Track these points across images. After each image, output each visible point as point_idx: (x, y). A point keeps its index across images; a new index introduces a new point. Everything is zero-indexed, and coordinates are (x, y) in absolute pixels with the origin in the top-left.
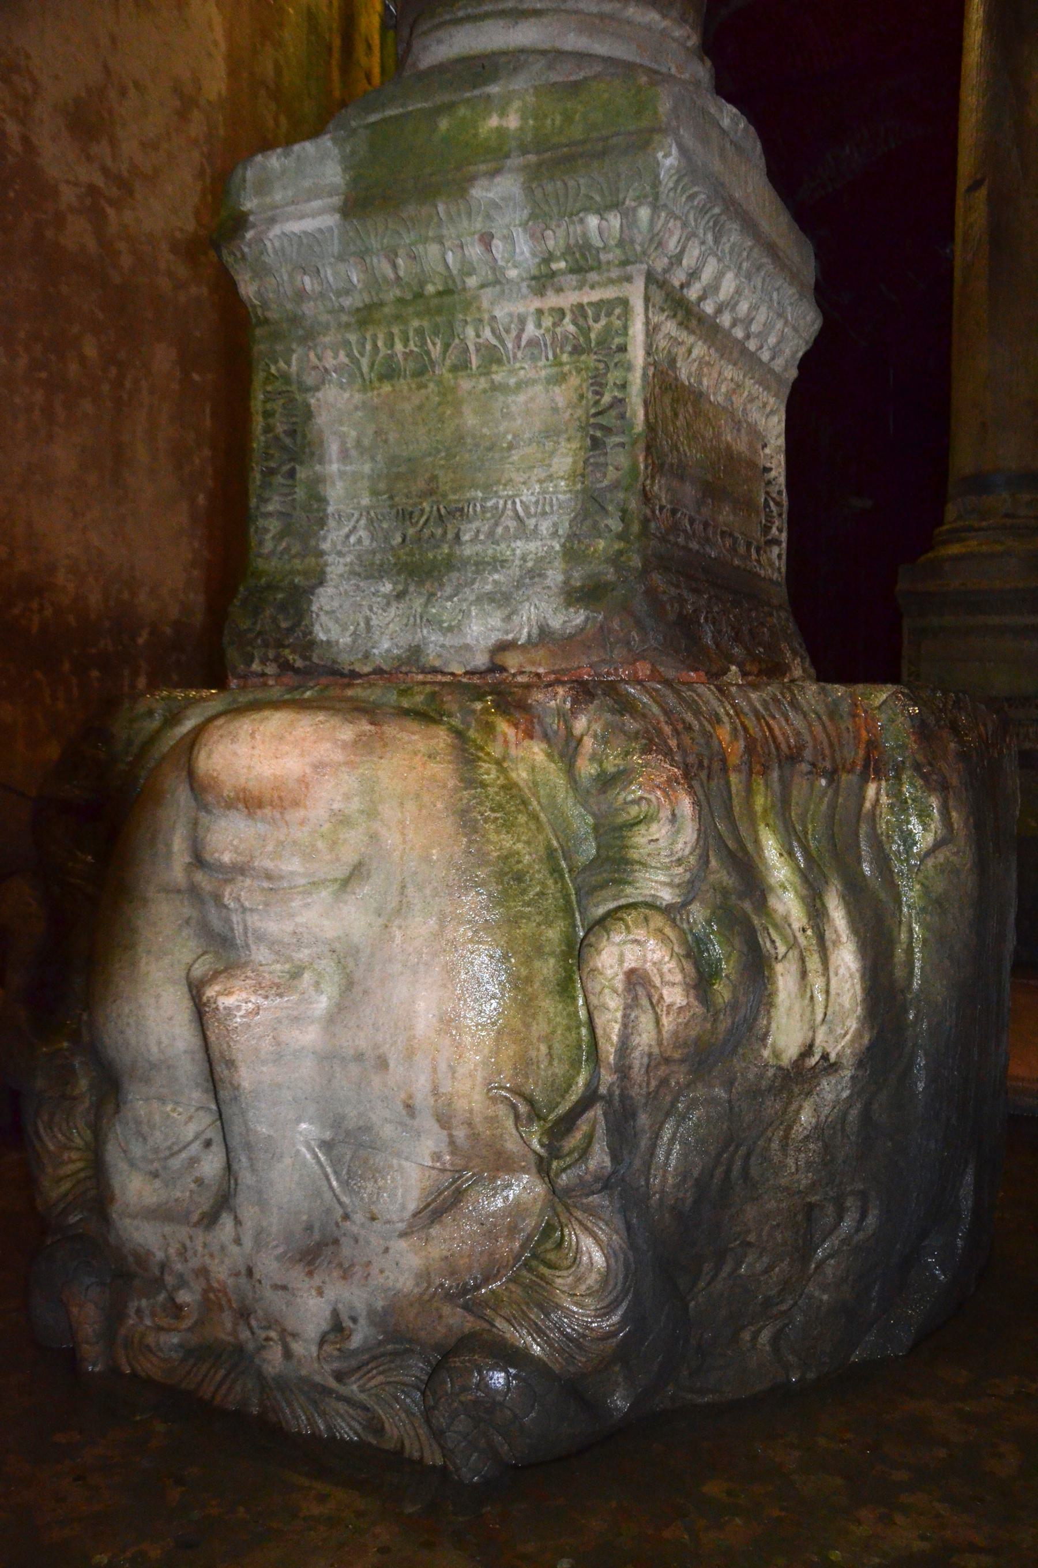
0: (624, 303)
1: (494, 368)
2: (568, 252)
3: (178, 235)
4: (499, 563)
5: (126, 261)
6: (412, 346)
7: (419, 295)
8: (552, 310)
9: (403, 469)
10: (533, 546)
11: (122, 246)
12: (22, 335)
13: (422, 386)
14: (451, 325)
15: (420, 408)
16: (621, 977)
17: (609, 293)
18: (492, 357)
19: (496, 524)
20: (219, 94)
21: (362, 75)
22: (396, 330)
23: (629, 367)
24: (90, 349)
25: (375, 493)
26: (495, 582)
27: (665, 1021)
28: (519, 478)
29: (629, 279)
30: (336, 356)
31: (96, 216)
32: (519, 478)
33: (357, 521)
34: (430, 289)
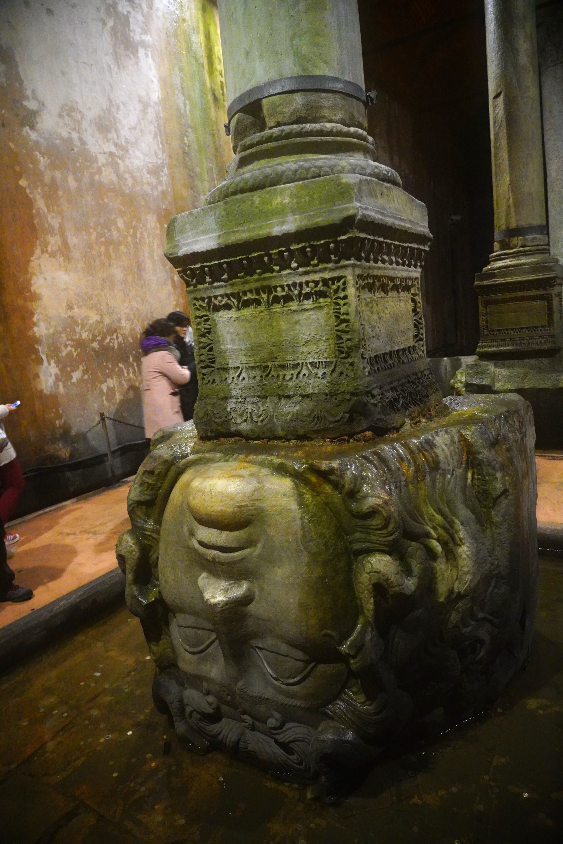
3: (150, 165)
5: (130, 182)
11: (127, 176)
12: (92, 224)
16: (371, 586)
20: (158, 97)
21: (219, 74)
24: (120, 223)
31: (114, 165)
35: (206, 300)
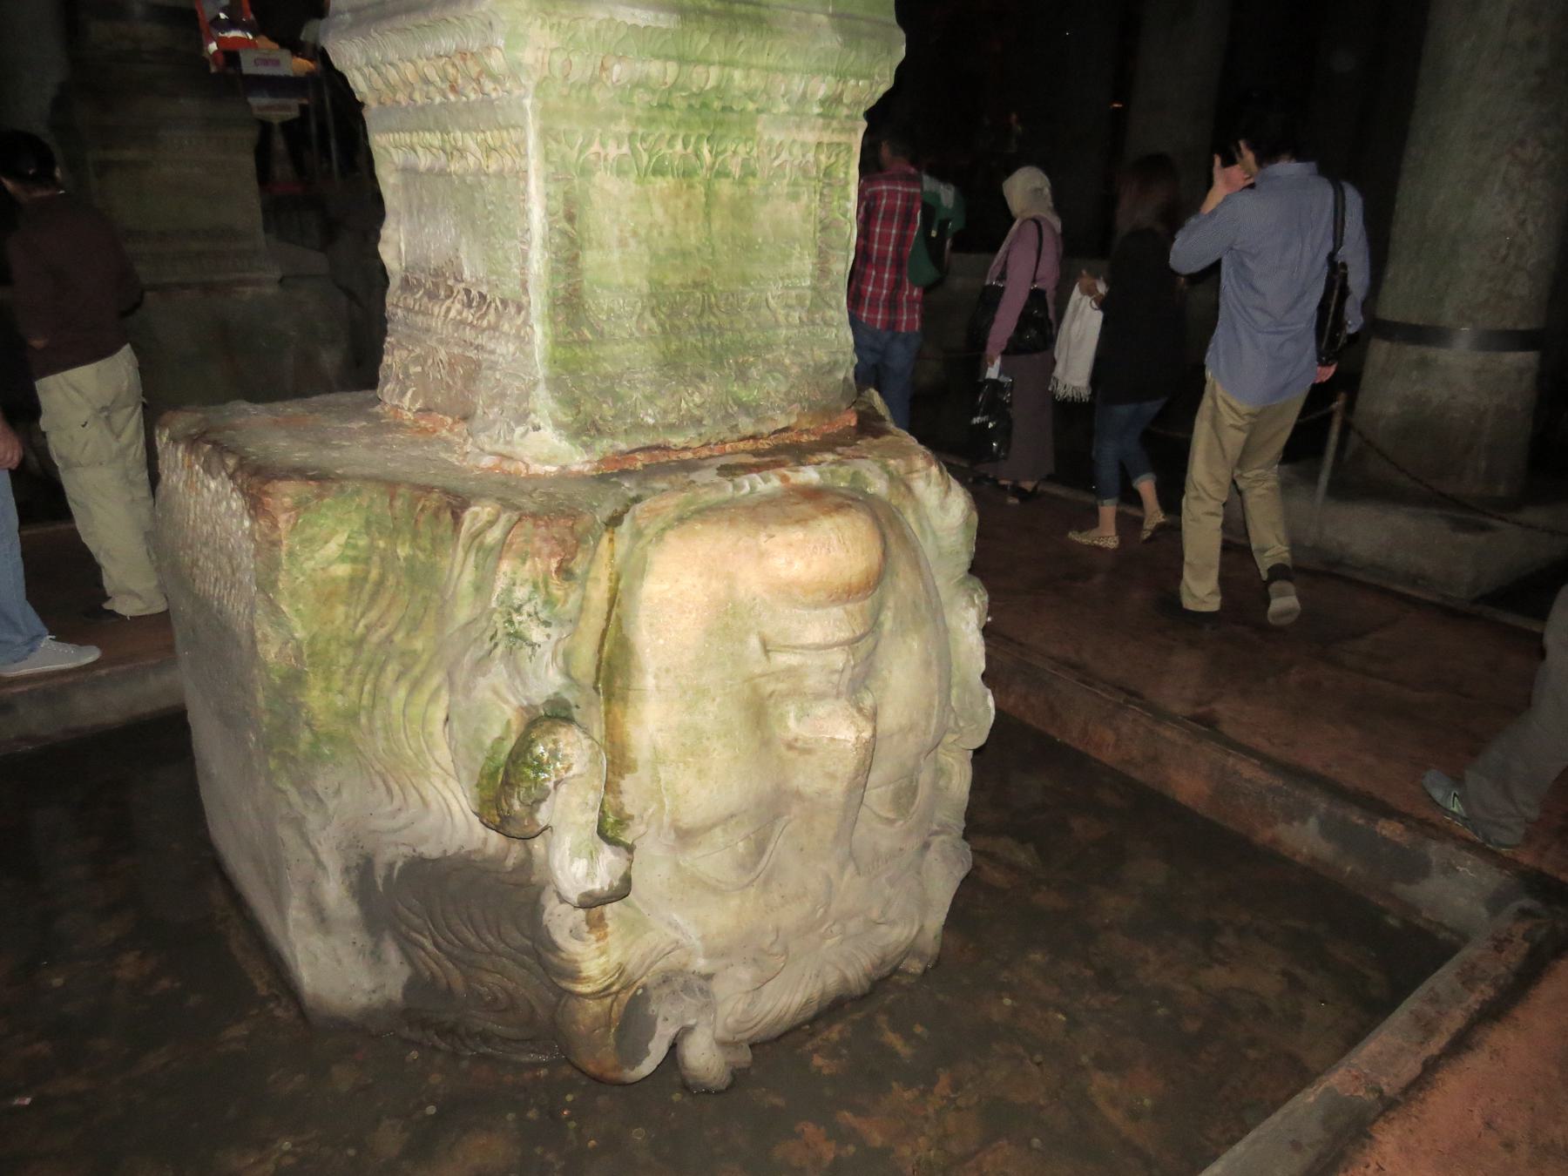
0: (849, 149)
1: (750, 180)
6: (690, 149)
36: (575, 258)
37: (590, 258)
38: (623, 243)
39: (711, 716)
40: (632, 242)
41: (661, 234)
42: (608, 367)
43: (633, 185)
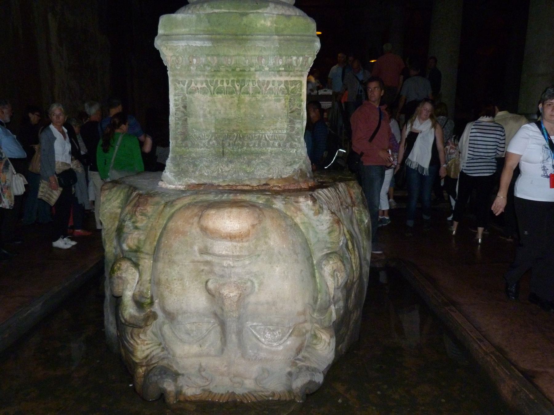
0: (301, 82)
1: (257, 95)
2: (285, 66)
4: (263, 154)
6: (230, 85)
7: (234, 70)
8: (278, 81)
9: (227, 122)
10: (273, 149)
13: (233, 97)
14: (243, 80)
15: (232, 103)
17: (297, 79)
18: (257, 92)
19: (260, 142)
22: (225, 79)
23: (302, 101)
25: (216, 129)
26: (262, 159)
27: (340, 280)
28: (266, 128)
29: (302, 76)
30: (202, 84)
32: (266, 128)
33: (212, 137)
34: (238, 69)
35: (187, 83)
36: (186, 120)
37: (190, 121)
38: (205, 116)
39: (176, 272)
40: (208, 115)
41: (220, 113)
42: (194, 155)
43: (208, 97)
